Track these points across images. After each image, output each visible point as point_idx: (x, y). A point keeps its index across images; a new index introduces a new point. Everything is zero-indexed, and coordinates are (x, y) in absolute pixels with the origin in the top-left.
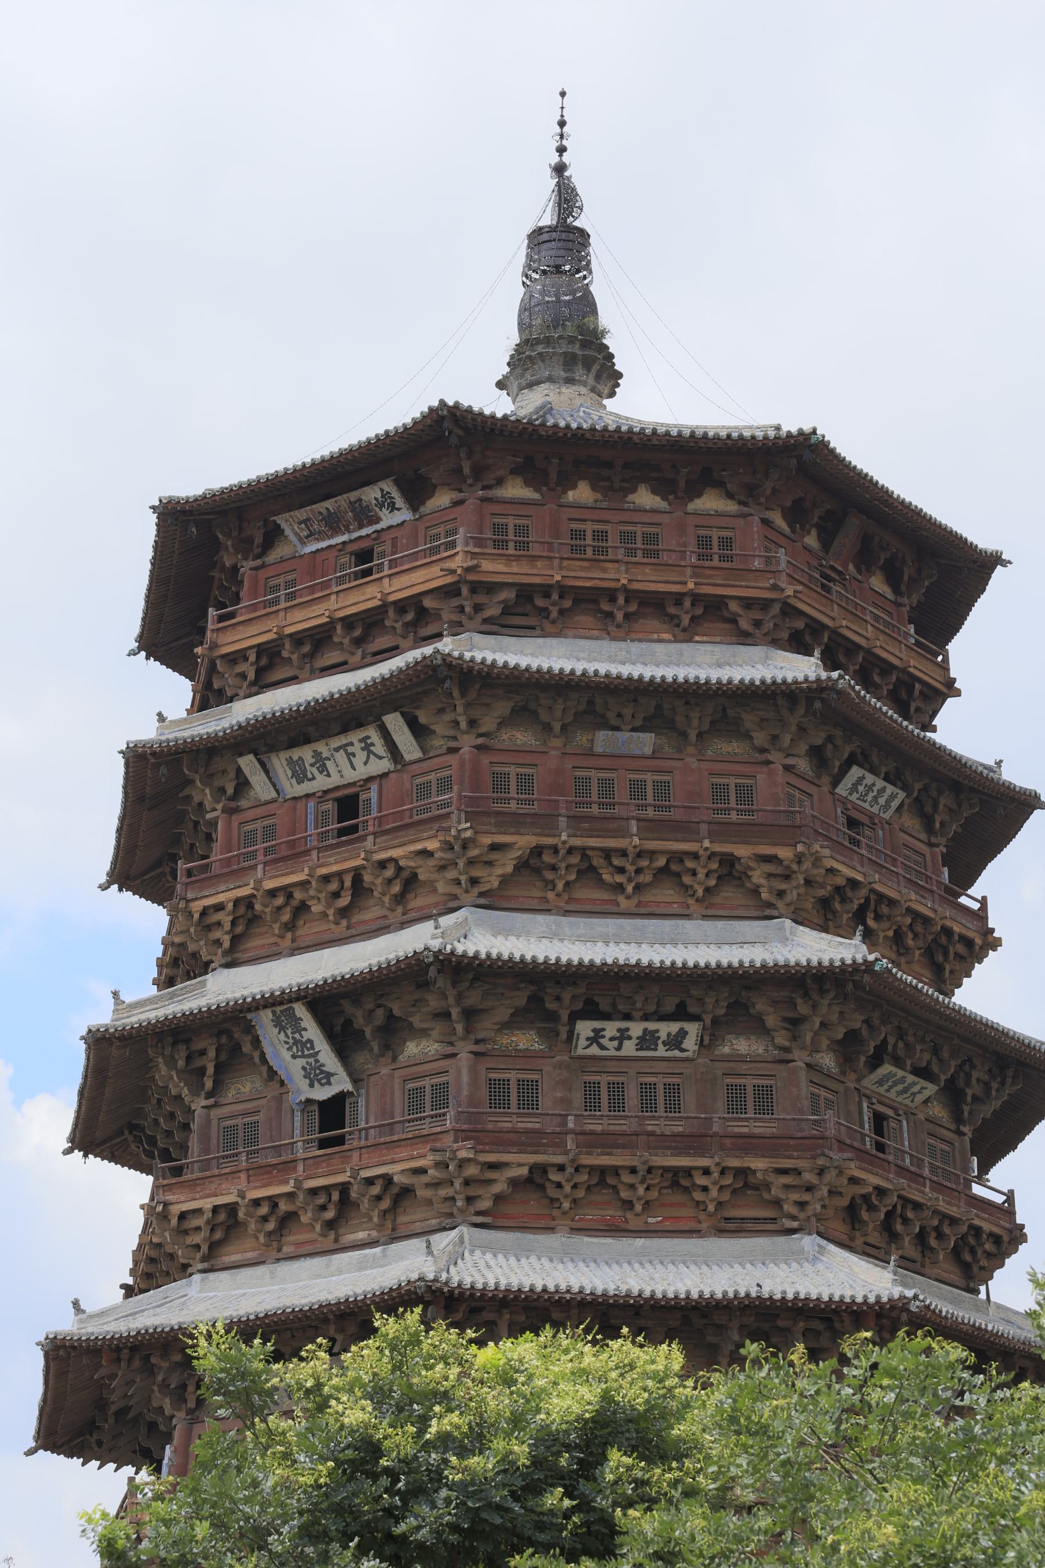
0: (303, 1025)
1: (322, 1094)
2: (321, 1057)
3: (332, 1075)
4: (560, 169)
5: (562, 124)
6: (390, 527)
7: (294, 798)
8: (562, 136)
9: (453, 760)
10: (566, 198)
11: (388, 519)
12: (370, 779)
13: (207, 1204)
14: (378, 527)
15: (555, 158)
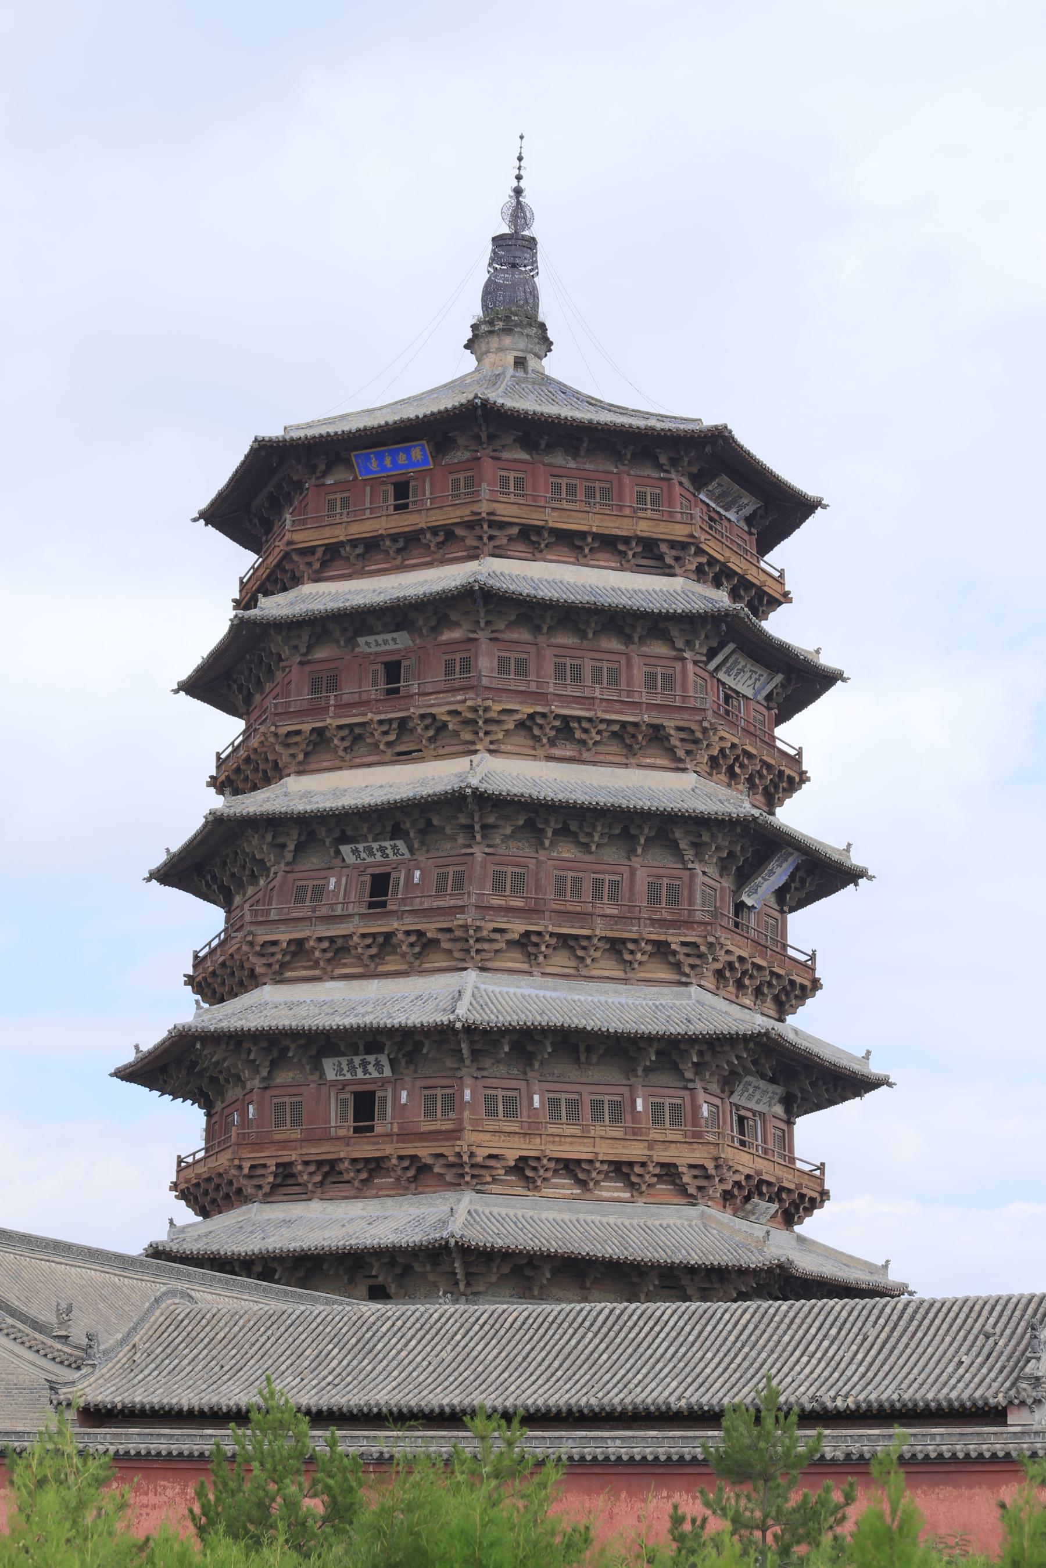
0: (785, 865)
1: (749, 902)
2: (766, 883)
3: (756, 892)
4: (518, 192)
5: (520, 159)
6: (729, 520)
7: (719, 680)
8: (519, 168)
9: (766, 712)
10: (519, 213)
11: (731, 515)
12: (744, 696)
13: (739, 952)
14: (727, 514)
15: (515, 183)
